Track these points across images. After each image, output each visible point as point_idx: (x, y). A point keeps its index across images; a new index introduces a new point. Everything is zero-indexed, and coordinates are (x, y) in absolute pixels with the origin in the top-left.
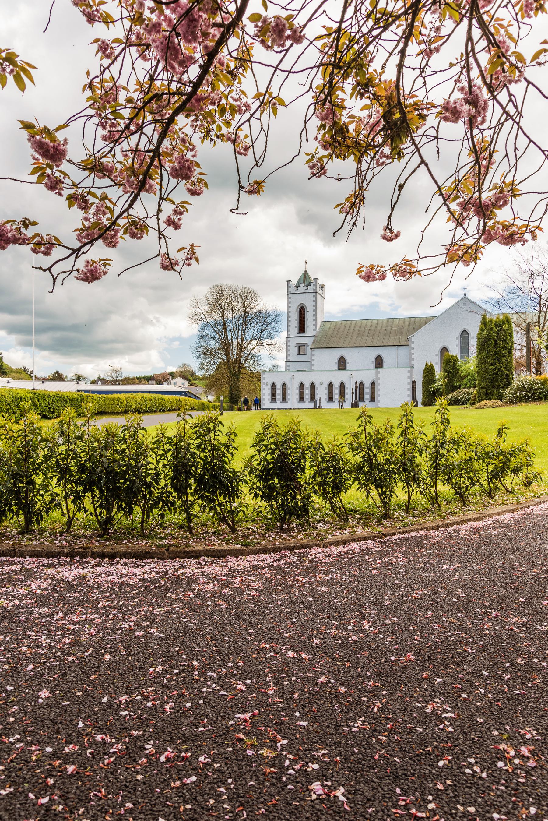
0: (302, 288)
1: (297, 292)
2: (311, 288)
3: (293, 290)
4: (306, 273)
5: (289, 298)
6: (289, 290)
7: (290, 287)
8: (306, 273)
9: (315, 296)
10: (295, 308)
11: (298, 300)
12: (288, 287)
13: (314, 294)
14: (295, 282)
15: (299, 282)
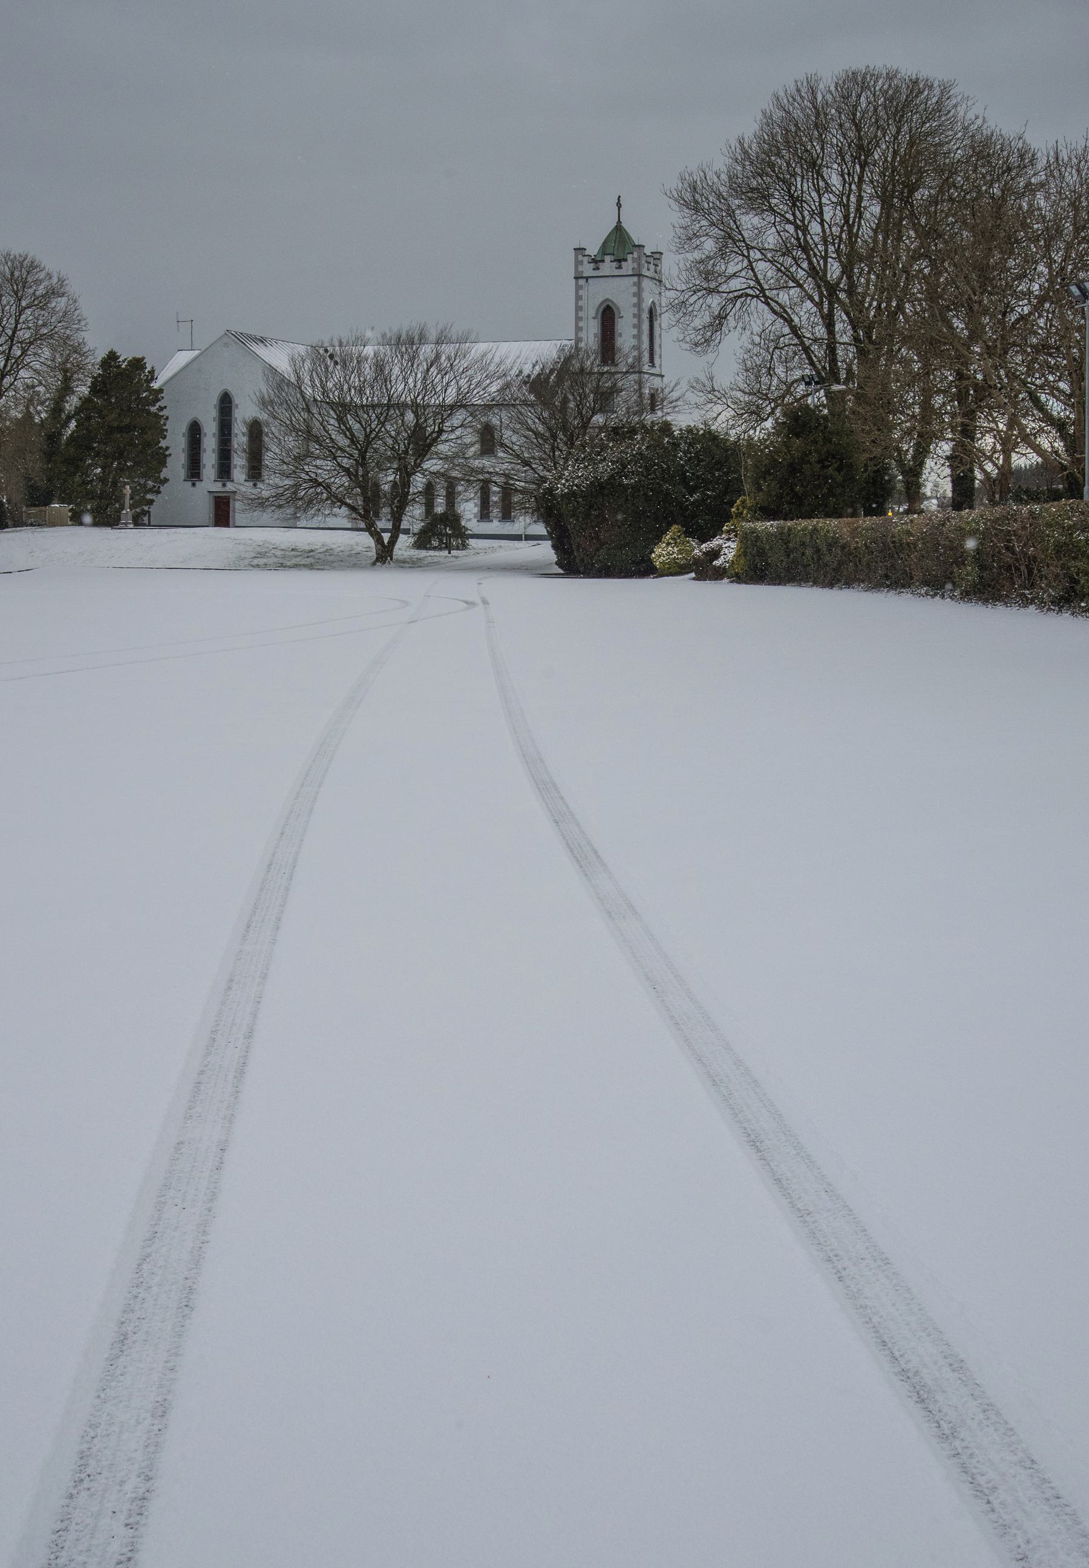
0: (608, 267)
1: (596, 273)
2: (628, 267)
3: (588, 269)
4: (619, 229)
5: (578, 288)
6: (580, 268)
7: (581, 263)
8: (619, 229)
9: (638, 285)
10: (591, 309)
11: (598, 292)
12: (578, 263)
13: (635, 279)
14: (593, 250)
15: (604, 250)
